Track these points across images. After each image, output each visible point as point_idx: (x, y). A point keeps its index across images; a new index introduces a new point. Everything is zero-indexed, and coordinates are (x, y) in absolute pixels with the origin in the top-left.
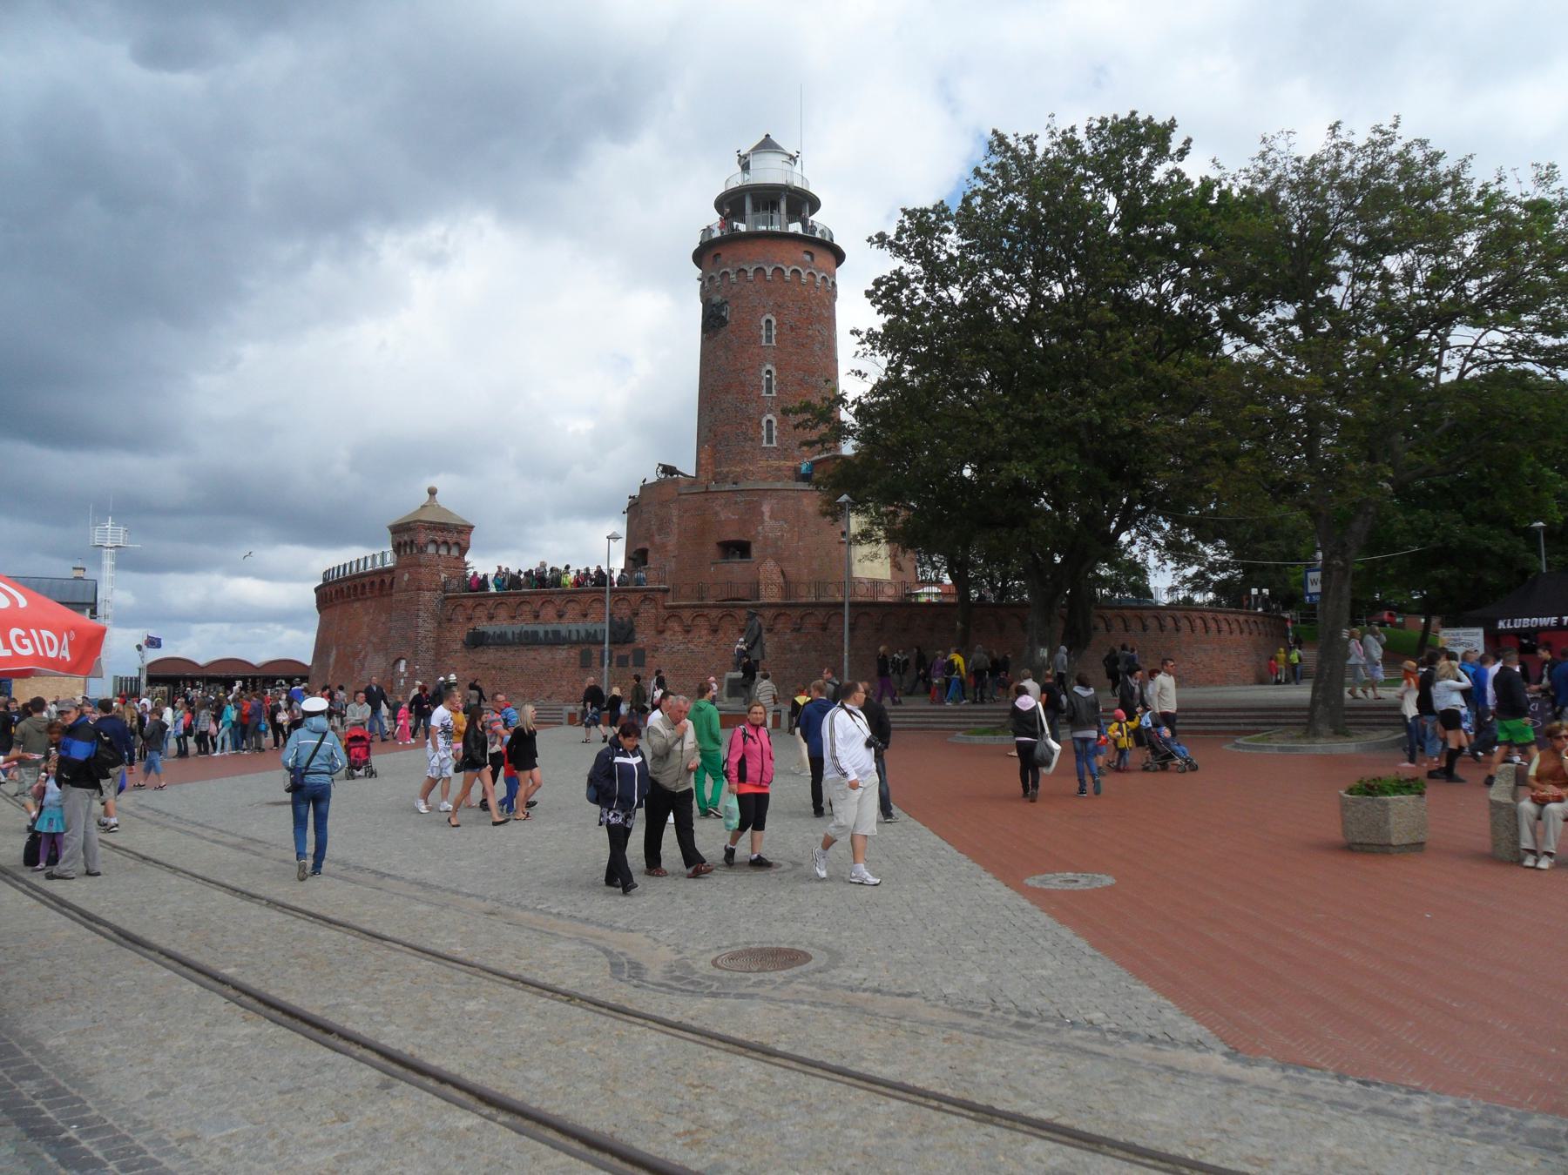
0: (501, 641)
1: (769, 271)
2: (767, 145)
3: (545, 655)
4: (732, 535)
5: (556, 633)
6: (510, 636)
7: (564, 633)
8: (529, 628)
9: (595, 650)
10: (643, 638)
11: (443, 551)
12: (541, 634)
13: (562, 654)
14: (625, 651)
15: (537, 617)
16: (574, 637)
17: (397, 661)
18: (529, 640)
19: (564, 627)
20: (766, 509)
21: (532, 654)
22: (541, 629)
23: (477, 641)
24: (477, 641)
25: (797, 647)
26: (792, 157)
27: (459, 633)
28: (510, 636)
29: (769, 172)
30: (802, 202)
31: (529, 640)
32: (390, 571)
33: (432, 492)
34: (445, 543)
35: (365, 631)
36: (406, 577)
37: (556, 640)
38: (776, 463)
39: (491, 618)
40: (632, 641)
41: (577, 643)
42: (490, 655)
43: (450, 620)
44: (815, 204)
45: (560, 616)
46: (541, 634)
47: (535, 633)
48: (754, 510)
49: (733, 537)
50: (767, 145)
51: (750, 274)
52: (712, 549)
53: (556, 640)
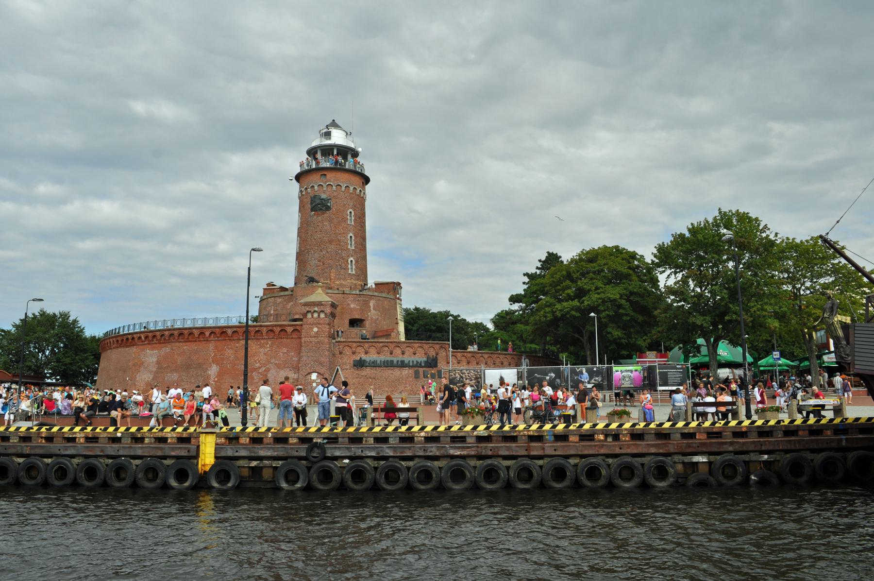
0: (374, 365)
3: (397, 372)
4: (357, 316)
5: (403, 362)
6: (379, 362)
7: (406, 362)
8: (389, 358)
9: (421, 370)
12: (395, 362)
13: (406, 371)
15: (391, 354)
16: (411, 364)
17: (310, 373)
18: (389, 365)
19: (407, 358)
20: (371, 305)
21: (390, 372)
22: (395, 360)
23: (360, 364)
24: (360, 364)
27: (348, 359)
28: (379, 362)
29: (338, 138)
31: (389, 365)
35: (263, 357)
36: (315, 330)
37: (403, 365)
38: (355, 282)
39: (366, 353)
40: (436, 366)
41: (412, 367)
42: (367, 371)
43: (341, 353)
45: (403, 354)
46: (395, 362)
47: (392, 361)
48: (366, 304)
49: (357, 317)
51: (343, 188)
52: (347, 322)
53: (403, 365)
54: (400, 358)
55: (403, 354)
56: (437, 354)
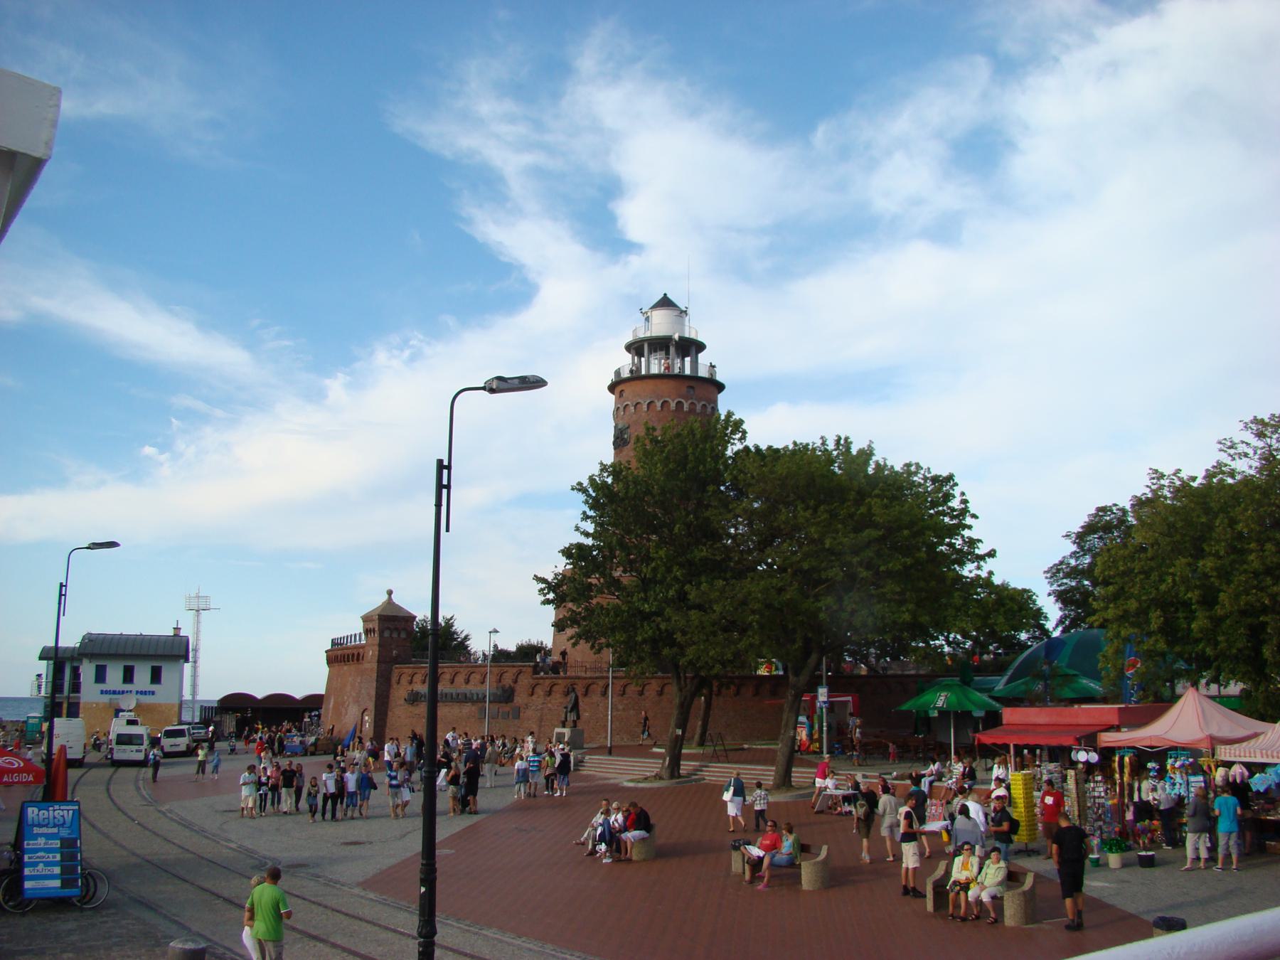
1: (659, 404)
2: (665, 303)
10: (520, 699)
11: (395, 635)
14: (506, 708)
25: (620, 707)
26: (682, 312)
29: (661, 325)
30: (690, 347)
32: (362, 647)
33: (390, 593)
34: (396, 629)
44: (700, 347)
45: (467, 681)
50: (665, 303)
51: (645, 407)
54: (464, 689)
55: (467, 681)
56: (516, 682)
